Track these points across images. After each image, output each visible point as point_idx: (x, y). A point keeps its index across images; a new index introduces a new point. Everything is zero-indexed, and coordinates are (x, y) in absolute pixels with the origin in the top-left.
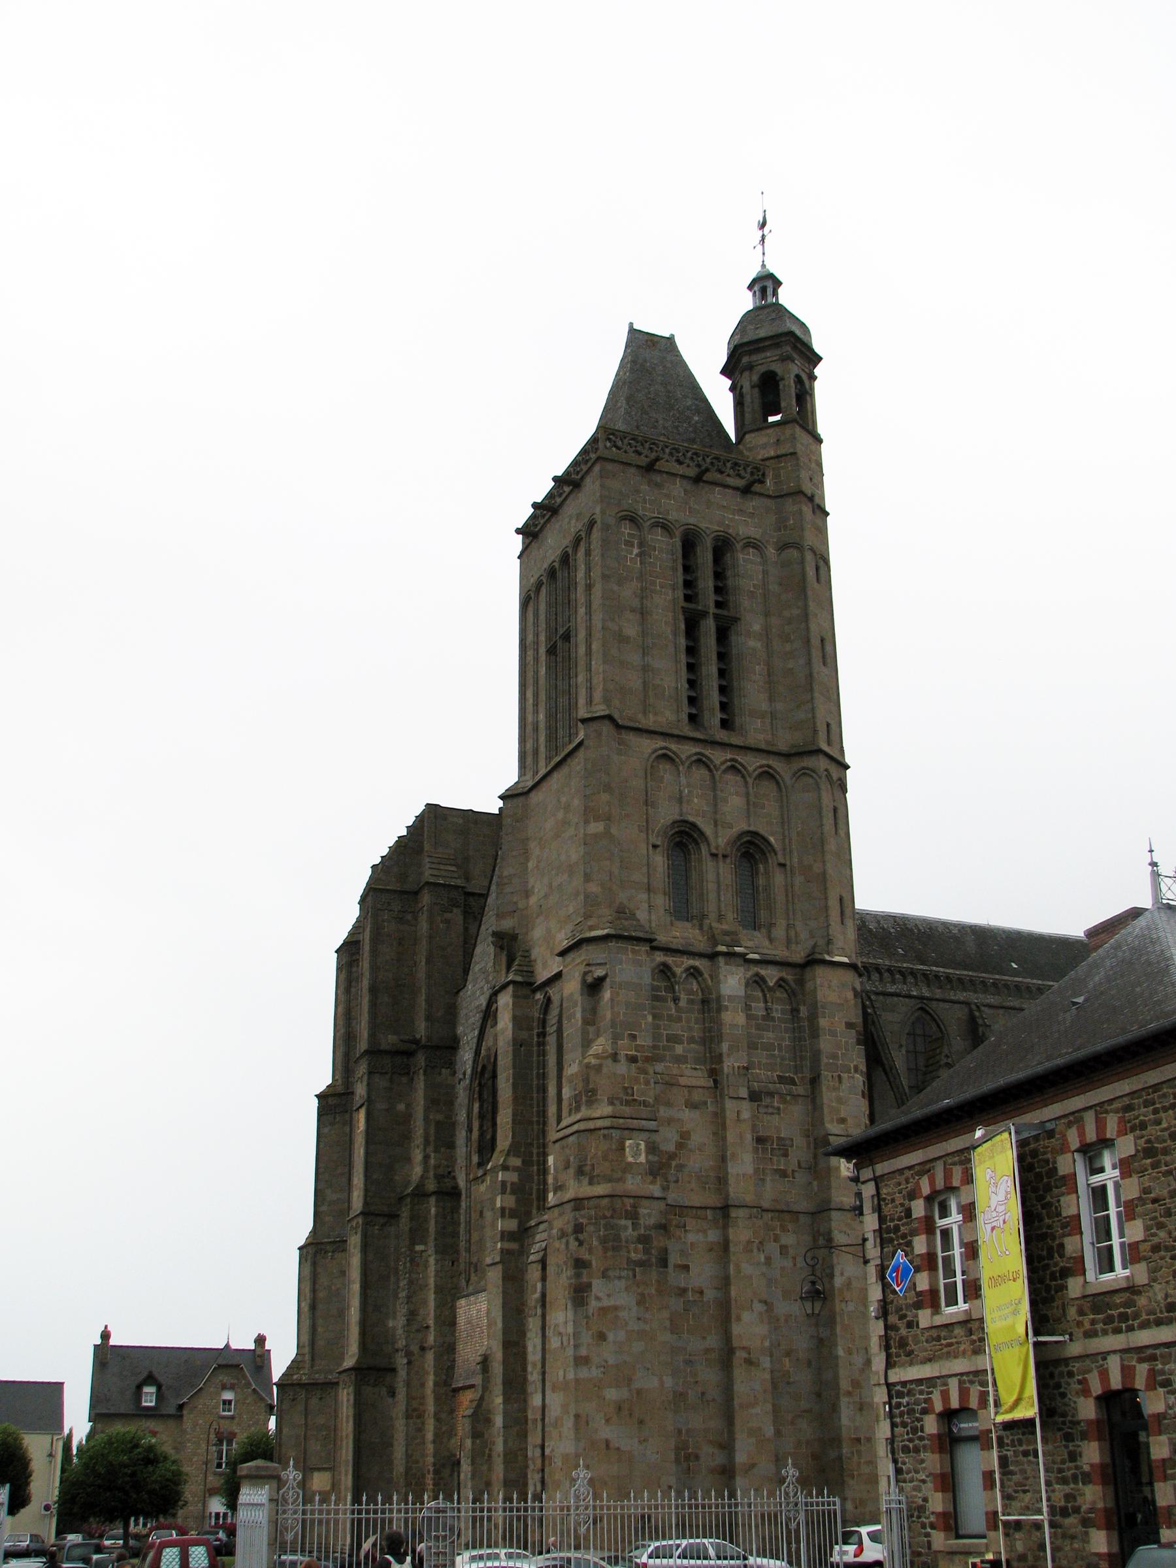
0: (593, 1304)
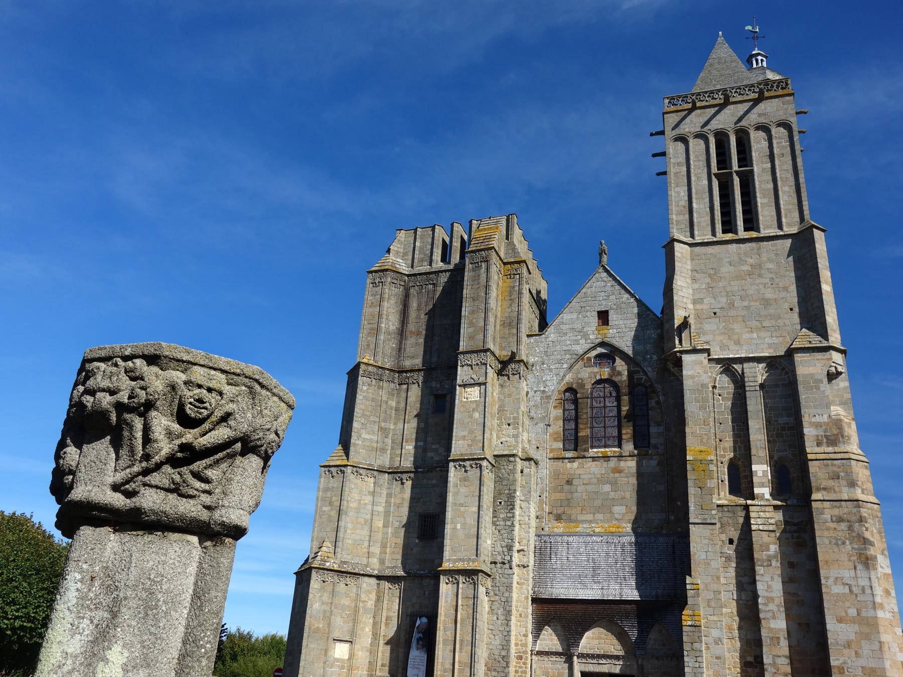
0: (880, 570)
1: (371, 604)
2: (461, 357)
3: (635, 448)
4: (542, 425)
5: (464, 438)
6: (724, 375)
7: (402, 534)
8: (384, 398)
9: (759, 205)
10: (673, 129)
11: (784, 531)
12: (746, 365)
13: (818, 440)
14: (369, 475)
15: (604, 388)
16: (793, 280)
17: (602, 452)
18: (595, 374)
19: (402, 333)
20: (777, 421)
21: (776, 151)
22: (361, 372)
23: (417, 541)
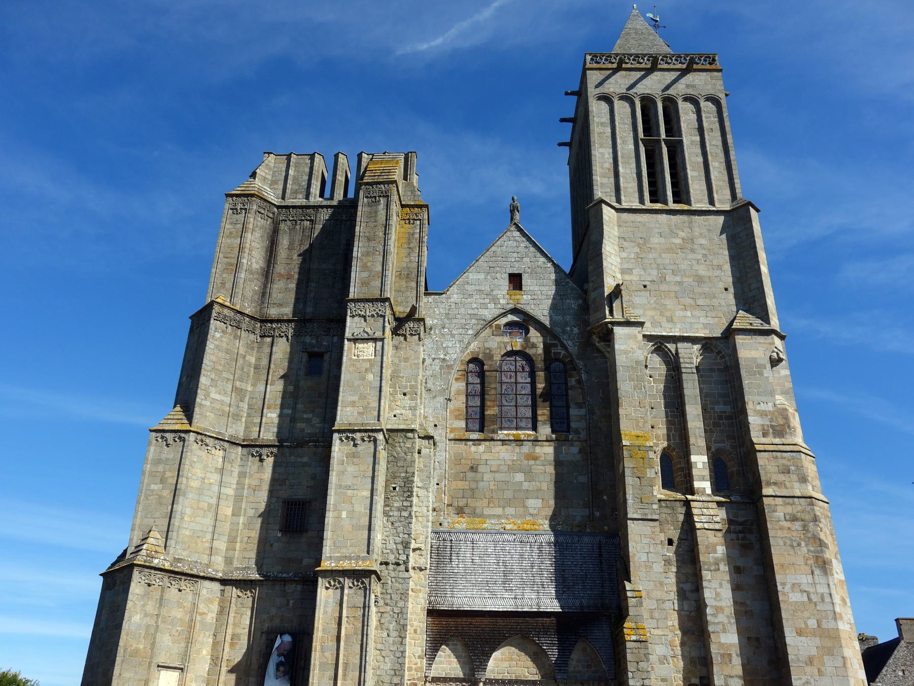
0: (836, 575)
1: (211, 617)
2: (351, 305)
3: (553, 432)
4: (441, 399)
5: (353, 404)
6: (655, 355)
7: (258, 526)
8: (242, 351)
9: (689, 177)
10: (597, 87)
11: (728, 531)
12: (680, 345)
13: (764, 430)
14: (218, 447)
15: (516, 361)
16: (727, 258)
17: (514, 435)
18: (505, 344)
19: (267, 274)
20: (714, 409)
21: (705, 125)
22: (214, 314)
23: (279, 535)
